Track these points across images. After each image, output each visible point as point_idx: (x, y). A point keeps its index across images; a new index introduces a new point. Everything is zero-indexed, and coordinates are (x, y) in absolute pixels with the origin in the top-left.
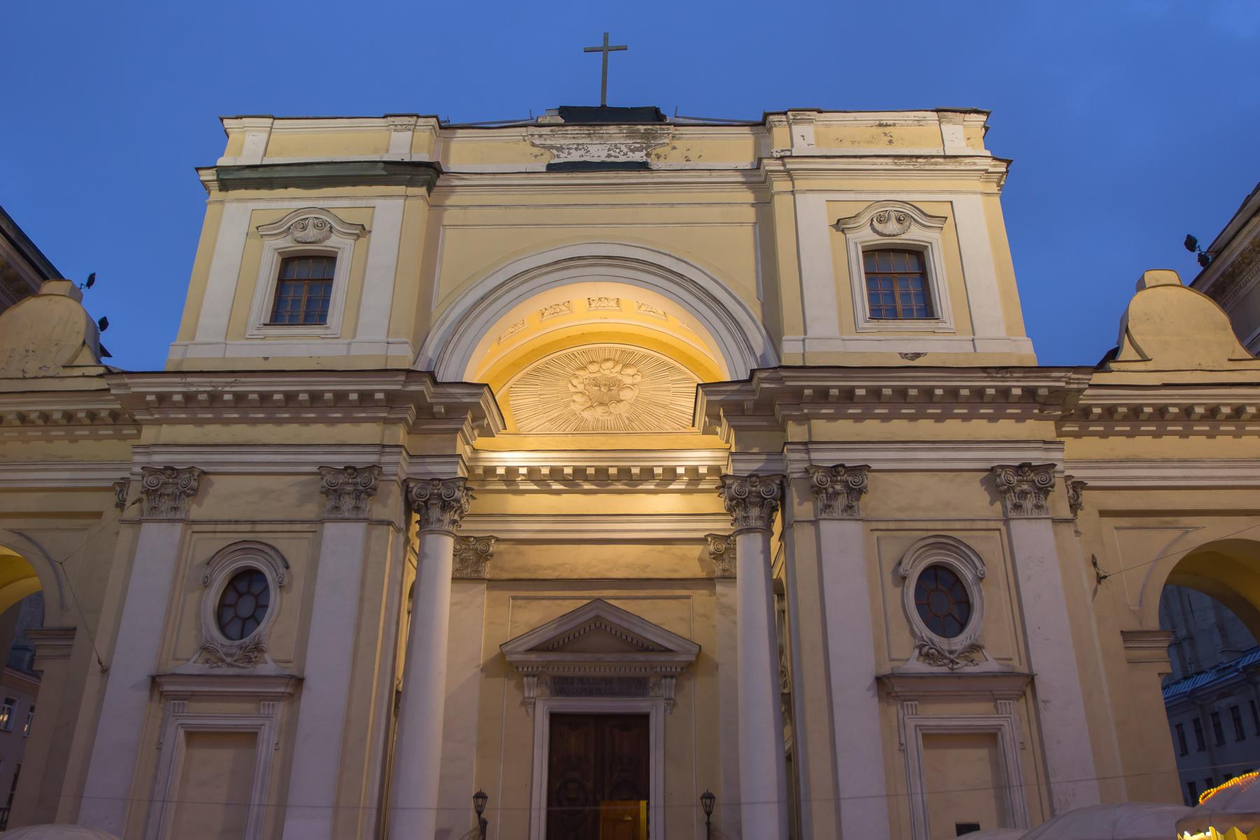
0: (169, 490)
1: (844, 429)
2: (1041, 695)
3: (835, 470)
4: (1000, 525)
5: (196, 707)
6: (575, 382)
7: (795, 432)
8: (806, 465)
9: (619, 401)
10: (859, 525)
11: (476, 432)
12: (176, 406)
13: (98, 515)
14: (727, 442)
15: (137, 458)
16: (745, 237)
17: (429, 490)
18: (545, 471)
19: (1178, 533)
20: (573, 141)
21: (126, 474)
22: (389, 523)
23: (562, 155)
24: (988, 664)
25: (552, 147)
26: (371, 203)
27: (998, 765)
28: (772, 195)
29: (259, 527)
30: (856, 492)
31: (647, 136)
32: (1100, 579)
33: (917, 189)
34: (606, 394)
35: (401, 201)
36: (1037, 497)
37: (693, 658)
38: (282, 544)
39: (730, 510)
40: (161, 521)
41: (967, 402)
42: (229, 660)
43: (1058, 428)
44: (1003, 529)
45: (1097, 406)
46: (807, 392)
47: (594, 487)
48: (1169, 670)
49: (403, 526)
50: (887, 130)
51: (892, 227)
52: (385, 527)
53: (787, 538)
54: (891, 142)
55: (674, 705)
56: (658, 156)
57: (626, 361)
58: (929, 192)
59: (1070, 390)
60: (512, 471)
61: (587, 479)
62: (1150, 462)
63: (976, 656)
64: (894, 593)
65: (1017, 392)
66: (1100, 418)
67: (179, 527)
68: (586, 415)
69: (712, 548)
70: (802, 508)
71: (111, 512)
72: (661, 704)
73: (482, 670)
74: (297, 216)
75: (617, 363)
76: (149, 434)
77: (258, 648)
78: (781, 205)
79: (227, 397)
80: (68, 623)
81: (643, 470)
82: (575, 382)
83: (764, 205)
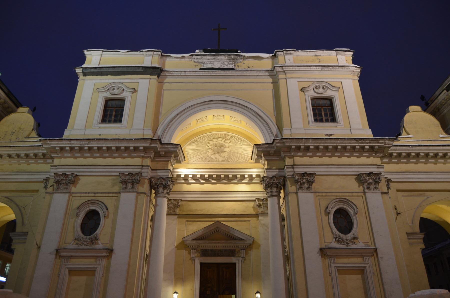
0: (64, 182)
1: (306, 160)
2: (380, 256)
3: (303, 175)
4: (362, 194)
6: (208, 145)
7: (288, 161)
8: (293, 173)
9: (224, 152)
10: (313, 194)
11: (175, 162)
12: (67, 152)
13: (37, 191)
14: (264, 165)
15: (52, 170)
16: (269, 94)
17: (159, 181)
18: (199, 176)
19: (425, 198)
20: (209, 61)
21: (48, 176)
22: (145, 193)
24: (360, 244)
25: (201, 63)
26: (138, 81)
27: (365, 280)
28: (279, 79)
29: (97, 195)
30: (311, 182)
31: (233, 59)
32: (398, 214)
33: (329, 77)
34: (219, 149)
35: (148, 80)
36: (375, 185)
37: (252, 243)
38: (105, 201)
39: (266, 189)
40: (61, 193)
41: (349, 151)
42: (85, 243)
43: (381, 160)
44: (364, 196)
45: (395, 153)
46: (293, 147)
47: (215, 182)
48: (424, 247)
49: (149, 194)
50: (318, 57)
51: (321, 90)
52: (143, 195)
53: (286, 199)
55: (245, 259)
56: (238, 66)
57: (226, 138)
58: (333, 79)
59: (386, 147)
60: (187, 176)
61: (213, 179)
62: (414, 173)
63: (355, 241)
64: (325, 218)
65: (367, 147)
66: (396, 157)
67: (68, 195)
68: (212, 156)
69: (257, 203)
70: (291, 188)
71: (42, 190)
72: (241, 259)
73: (176, 247)
74: (111, 85)
75: (223, 139)
76: (57, 162)
77: (96, 239)
78: (282, 83)
79: (86, 148)
80: (25, 230)
81: (233, 176)
82: (208, 145)
83: (276, 83)
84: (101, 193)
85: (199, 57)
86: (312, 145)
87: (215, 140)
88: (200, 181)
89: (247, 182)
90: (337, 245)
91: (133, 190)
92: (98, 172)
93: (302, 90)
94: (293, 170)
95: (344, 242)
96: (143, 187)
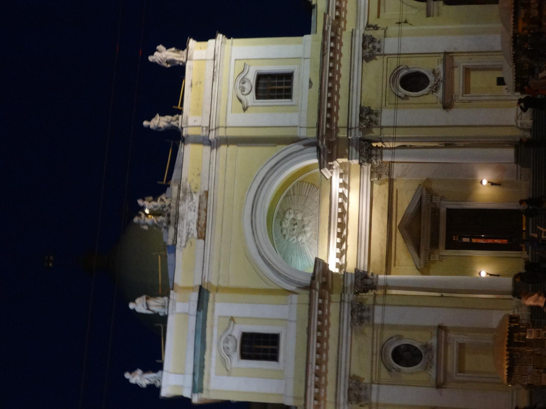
2: (453, 51)
5: (449, 369)
7: (342, 134)
8: (357, 130)
23: (192, 232)
29: (375, 352)
30: (370, 111)
31: (185, 193)
32: (406, 22)
36: (376, 42)
44: (387, 56)
45: (336, 13)
50: (194, 84)
54: (200, 83)
55: (443, 197)
61: (342, 233)
63: (437, 72)
64: (411, 100)
66: (340, 13)
69: (376, 179)
72: (443, 202)
78: (231, 133)
84: (373, 347)
85: (179, 240)
86: (327, 105)
88: (343, 250)
89: (347, 190)
90: (440, 91)
91: (371, 309)
92: (346, 354)
93: (245, 109)
94: (353, 130)
95: (437, 83)
96: (367, 299)
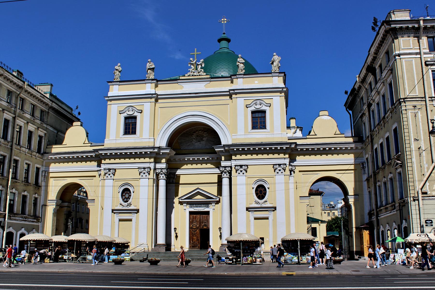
6: (193, 136)
13: (95, 176)
24: (268, 205)
75: (202, 131)
87: (197, 132)
